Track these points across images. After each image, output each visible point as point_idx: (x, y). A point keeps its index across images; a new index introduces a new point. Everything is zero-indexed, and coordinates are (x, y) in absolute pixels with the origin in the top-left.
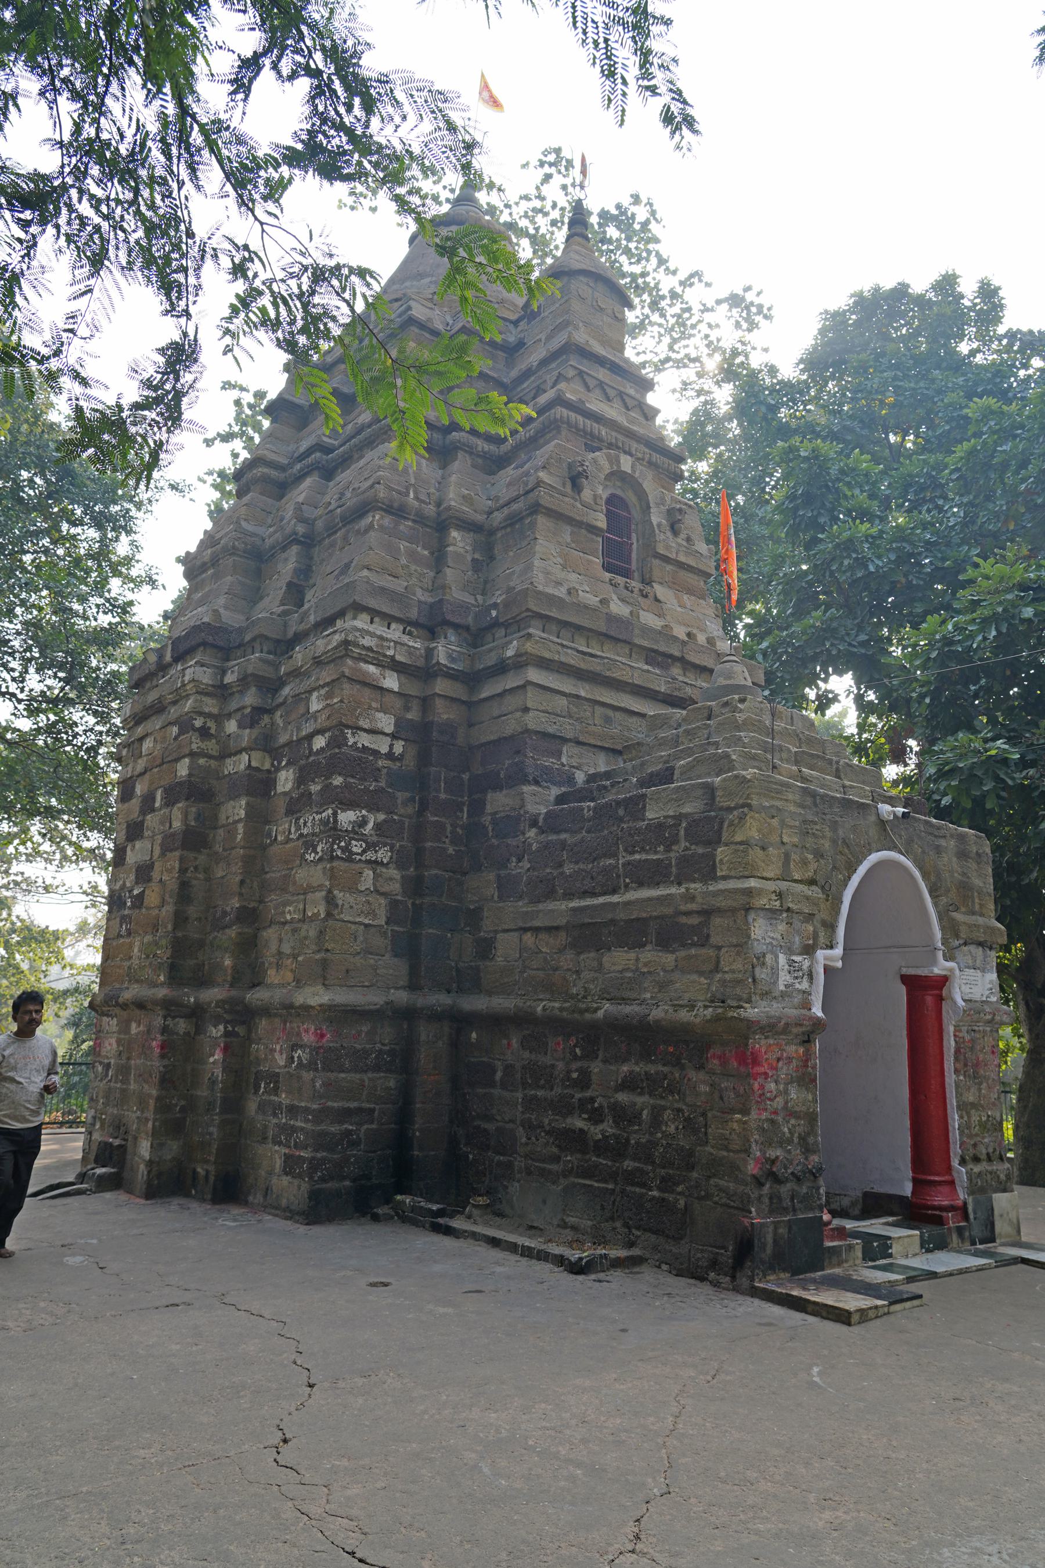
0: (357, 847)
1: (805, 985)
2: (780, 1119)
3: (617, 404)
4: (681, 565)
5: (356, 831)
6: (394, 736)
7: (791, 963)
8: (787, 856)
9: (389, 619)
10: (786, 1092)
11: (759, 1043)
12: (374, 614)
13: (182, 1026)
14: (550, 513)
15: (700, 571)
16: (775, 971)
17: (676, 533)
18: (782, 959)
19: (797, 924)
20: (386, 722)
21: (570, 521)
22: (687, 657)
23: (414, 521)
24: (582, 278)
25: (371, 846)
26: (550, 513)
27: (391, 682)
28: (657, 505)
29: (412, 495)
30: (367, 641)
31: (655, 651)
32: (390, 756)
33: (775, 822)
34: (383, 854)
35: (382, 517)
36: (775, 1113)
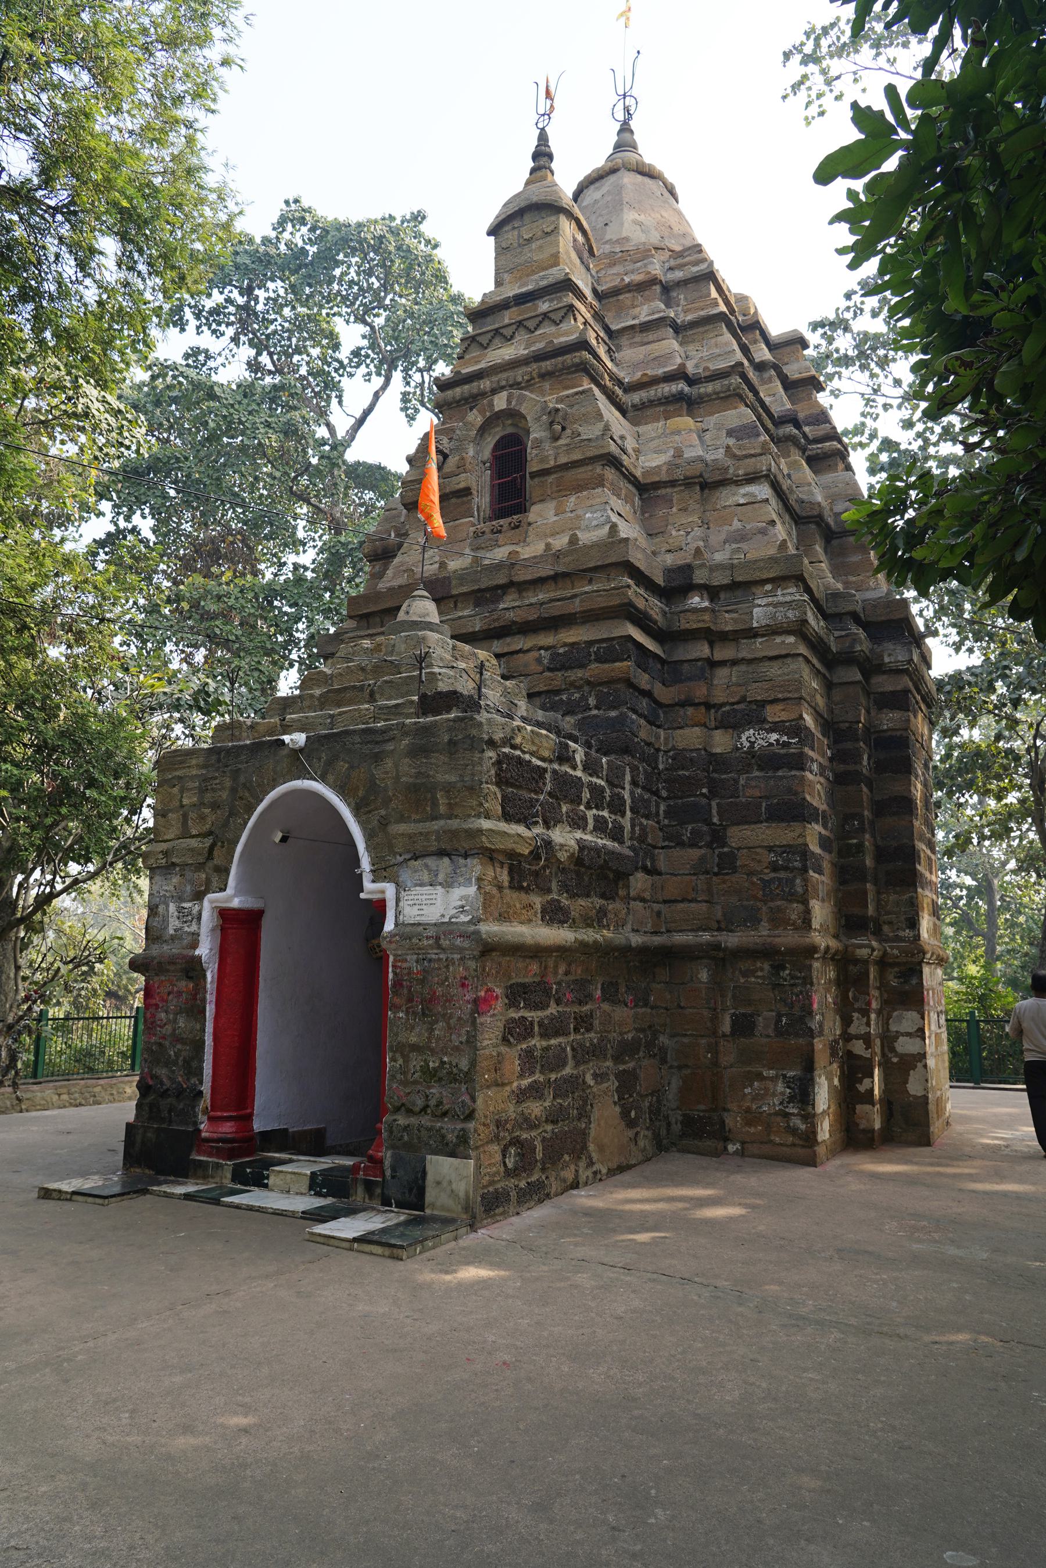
1: (194, 928)
2: (167, 1043)
7: (180, 909)
8: (185, 816)
10: (175, 1021)
15: (591, 458)
18: (172, 907)
19: (189, 874)
22: (516, 579)
24: (506, 228)
31: (479, 590)
33: (175, 790)
36: (164, 1038)
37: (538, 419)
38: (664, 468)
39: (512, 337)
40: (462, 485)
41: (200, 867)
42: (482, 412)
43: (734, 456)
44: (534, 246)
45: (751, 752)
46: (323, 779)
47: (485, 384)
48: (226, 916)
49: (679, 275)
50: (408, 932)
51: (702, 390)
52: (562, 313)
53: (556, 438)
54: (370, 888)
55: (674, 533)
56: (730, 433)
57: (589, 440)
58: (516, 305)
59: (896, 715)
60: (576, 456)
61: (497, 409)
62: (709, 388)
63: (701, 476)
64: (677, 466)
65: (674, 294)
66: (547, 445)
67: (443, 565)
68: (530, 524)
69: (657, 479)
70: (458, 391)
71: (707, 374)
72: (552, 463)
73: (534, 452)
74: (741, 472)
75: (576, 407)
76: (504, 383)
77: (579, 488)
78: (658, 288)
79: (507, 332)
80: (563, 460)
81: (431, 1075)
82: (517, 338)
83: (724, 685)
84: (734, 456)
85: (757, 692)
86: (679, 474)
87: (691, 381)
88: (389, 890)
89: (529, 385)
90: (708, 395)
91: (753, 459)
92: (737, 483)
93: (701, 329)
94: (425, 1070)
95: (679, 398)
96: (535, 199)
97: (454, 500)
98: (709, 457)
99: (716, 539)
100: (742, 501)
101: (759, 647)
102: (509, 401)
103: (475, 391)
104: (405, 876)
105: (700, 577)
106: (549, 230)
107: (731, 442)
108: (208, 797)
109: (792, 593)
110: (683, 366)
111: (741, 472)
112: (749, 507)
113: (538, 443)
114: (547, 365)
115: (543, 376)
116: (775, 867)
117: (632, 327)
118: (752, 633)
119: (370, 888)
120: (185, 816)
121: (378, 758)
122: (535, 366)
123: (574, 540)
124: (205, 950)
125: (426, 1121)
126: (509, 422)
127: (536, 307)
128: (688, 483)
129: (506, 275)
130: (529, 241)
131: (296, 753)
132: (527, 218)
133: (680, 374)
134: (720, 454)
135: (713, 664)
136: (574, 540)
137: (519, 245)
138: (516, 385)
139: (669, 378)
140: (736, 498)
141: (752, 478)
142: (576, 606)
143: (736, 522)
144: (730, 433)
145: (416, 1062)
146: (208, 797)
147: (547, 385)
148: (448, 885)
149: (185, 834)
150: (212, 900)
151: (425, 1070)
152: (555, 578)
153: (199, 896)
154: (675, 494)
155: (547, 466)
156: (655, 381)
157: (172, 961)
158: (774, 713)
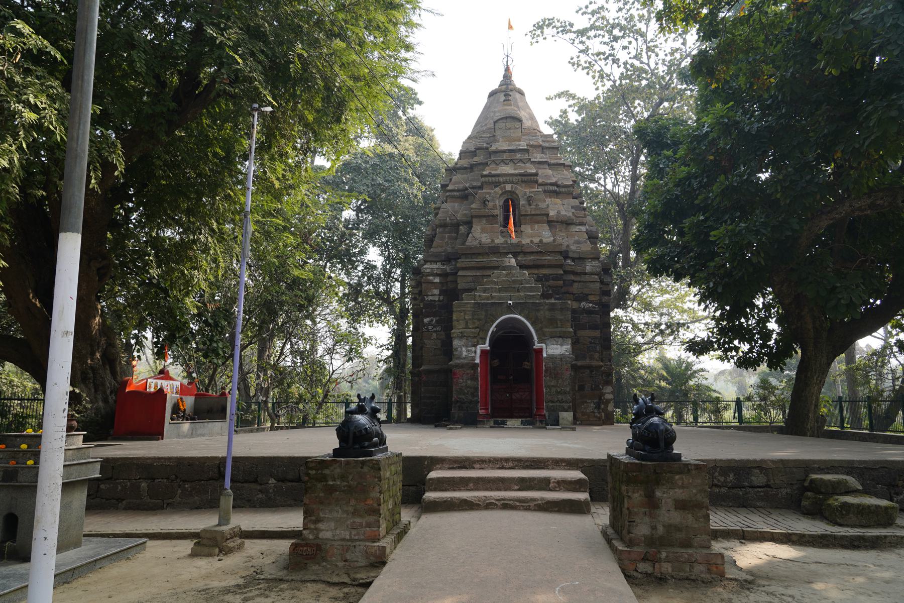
0: (430, 328)
1: (473, 355)
3: (511, 164)
5: (430, 323)
6: (440, 295)
8: (467, 323)
9: (436, 262)
11: (457, 371)
12: (431, 262)
13: (417, 379)
14: (476, 217)
16: (461, 352)
17: (530, 205)
18: (464, 349)
20: (436, 292)
21: (484, 216)
25: (434, 327)
26: (476, 217)
27: (437, 280)
30: (428, 271)
32: (439, 300)
34: (439, 328)
41: (475, 337)
42: (501, 189)
45: (584, 309)
46: (520, 314)
47: (501, 179)
48: (483, 351)
49: (547, 145)
50: (552, 358)
53: (530, 205)
54: (537, 345)
56: (572, 207)
59: (606, 298)
62: (563, 190)
66: (527, 207)
67: (493, 241)
70: (490, 179)
77: (538, 222)
81: (558, 393)
83: (576, 288)
85: (586, 291)
86: (560, 219)
87: (558, 186)
88: (544, 346)
89: (517, 183)
92: (576, 224)
94: (556, 391)
95: (555, 192)
99: (571, 241)
101: (587, 278)
104: (548, 342)
105: (571, 255)
108: (476, 317)
109: (596, 263)
113: (523, 205)
114: (524, 178)
116: (591, 343)
118: (585, 274)
119: (537, 345)
120: (467, 323)
121: (538, 310)
123: (541, 241)
124: (478, 361)
125: (558, 404)
128: (562, 222)
131: (509, 306)
132: (508, 120)
133: (555, 184)
134: (571, 214)
135: (574, 281)
136: (541, 241)
138: (512, 182)
139: (551, 184)
141: (581, 224)
142: (546, 263)
144: (572, 207)
145: (554, 390)
146: (476, 317)
148: (561, 345)
149: (467, 327)
150: (479, 348)
151: (556, 391)
152: (538, 253)
153: (475, 346)
154: (558, 225)
156: (547, 184)
157: (467, 364)
158: (591, 298)
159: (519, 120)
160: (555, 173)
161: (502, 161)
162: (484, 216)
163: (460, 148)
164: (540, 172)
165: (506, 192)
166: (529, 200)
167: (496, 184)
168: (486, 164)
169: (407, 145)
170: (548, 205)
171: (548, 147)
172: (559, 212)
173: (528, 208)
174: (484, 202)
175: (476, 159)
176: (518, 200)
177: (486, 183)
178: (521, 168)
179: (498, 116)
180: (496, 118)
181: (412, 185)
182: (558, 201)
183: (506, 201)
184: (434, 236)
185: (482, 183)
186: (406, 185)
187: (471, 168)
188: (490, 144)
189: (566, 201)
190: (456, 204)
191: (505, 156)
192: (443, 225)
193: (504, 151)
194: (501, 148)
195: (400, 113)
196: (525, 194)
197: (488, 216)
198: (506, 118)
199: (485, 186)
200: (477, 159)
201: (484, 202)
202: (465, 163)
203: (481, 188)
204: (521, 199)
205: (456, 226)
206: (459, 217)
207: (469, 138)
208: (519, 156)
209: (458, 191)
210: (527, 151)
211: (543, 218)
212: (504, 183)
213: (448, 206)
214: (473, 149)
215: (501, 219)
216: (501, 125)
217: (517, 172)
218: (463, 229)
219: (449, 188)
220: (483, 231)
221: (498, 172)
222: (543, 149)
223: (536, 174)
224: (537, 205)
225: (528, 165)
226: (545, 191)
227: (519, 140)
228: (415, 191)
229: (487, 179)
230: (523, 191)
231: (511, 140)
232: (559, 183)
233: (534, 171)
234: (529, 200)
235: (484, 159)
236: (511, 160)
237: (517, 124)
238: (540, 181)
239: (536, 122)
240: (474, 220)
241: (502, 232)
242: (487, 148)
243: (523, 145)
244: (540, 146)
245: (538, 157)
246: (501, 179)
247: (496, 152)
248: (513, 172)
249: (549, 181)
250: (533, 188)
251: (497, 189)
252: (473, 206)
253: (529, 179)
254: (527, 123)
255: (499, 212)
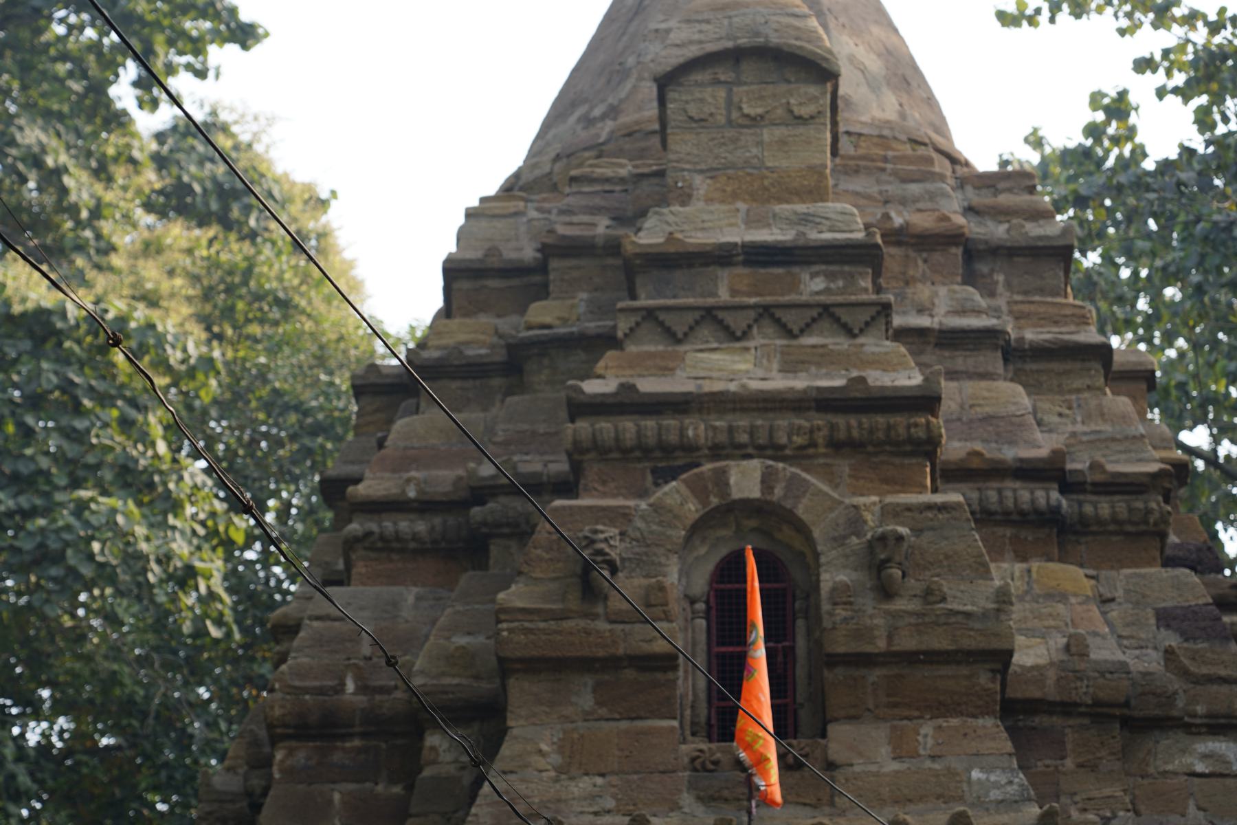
4: (911, 658)
14: (534, 666)
17: (886, 592)
21: (586, 665)
23: (364, 735)
26: (534, 666)
28: (840, 541)
29: (350, 686)
35: (291, 752)
37: (840, 541)
38: (1052, 675)
39: (745, 335)
40: (660, 646)
42: (699, 490)
43: (1185, 673)
44: (766, 134)
47: (696, 429)
49: (998, 231)
51: (1088, 509)
52: (865, 316)
53: (886, 592)
55: (1075, 814)
56: (1165, 618)
57: (968, 615)
58: (747, 263)
60: (939, 641)
61: (736, 494)
62: (1104, 507)
63: (1127, 704)
64: (1079, 676)
65: (983, 268)
68: (831, 766)
69: (1036, 694)
70: (629, 426)
71: (1099, 477)
72: (882, 645)
73: (841, 612)
74: (1200, 709)
75: (928, 536)
76: (744, 438)
77: (941, 707)
78: (958, 251)
79: (737, 322)
80: (908, 642)
82: (756, 341)
84: (1185, 673)
86: (1082, 692)
87: (1069, 484)
89: (800, 456)
90: (1099, 521)
91: (1225, 689)
93: (1056, 366)
95: (1049, 519)
96: (775, 40)
97: (629, 674)
98: (1136, 666)
100: (1200, 768)
102: (767, 480)
103: (673, 438)
106: (805, 111)
107: (1171, 639)
110: (1058, 456)
111: (1200, 709)
112: (1213, 781)
113: (842, 595)
115: (837, 446)
117: (922, 332)
122: (819, 420)
126: (753, 523)
127: (794, 286)
129: (698, 180)
130: (755, 121)
132: (749, 69)
133: (1047, 471)
134: (1151, 662)
137: (730, 123)
138: (771, 449)
139: (1028, 472)
140: (1188, 760)
143: (1192, 809)
144: (1165, 618)
147: (844, 466)
155: (869, 649)
156: (996, 471)
159: (820, 71)
160: (1050, 407)
161: (710, 315)
162: (586, 665)
163: (449, 246)
164: (948, 388)
165: (731, 512)
166: (881, 561)
167: (668, 460)
168: (610, 341)
169: (147, 273)
170: (1003, 598)
171: (1010, 234)
172: (1075, 648)
173: (874, 615)
174: (588, 579)
175: (545, 314)
176: (811, 562)
177: (600, 450)
178: (823, 358)
179: (680, 39)
180: (673, 58)
181: (162, 505)
182: (1071, 576)
183: (731, 569)
184: (256, 807)
185: (578, 454)
186: (125, 511)
187: (513, 365)
188: (632, 218)
189: (1121, 579)
190: (410, 595)
191: (724, 288)
192: (317, 726)
193: (722, 257)
194: (699, 238)
195: (123, 92)
196: (855, 522)
197: (613, 663)
198: (735, 56)
199: (592, 471)
200: (545, 314)
201: (587, 568)
202: (479, 336)
203: (567, 487)
204: (829, 554)
205: (398, 731)
206: (423, 668)
207: (512, 187)
208: (813, 285)
209: (424, 506)
210: (861, 255)
211: (967, 674)
212: (717, 452)
213: (358, 601)
214: (528, 253)
215: (691, 683)
216: (704, 97)
217: (800, 383)
218: (442, 748)
219: (371, 487)
220: (575, 760)
221: (678, 384)
222: (973, 258)
223: (926, 401)
224: (930, 595)
225: (875, 344)
226: (984, 517)
227: (817, 193)
228: (181, 548)
229: (606, 427)
230: (840, 505)
231: (765, 191)
232: (1078, 464)
233: (910, 379)
234: (881, 561)
235: (599, 310)
236: (766, 312)
237: (805, 97)
238: (953, 449)
239: (930, 101)
240: (520, 690)
241: (699, 766)
242: (613, 247)
243: (844, 217)
244: (954, 238)
245: (941, 302)
246: (696, 429)
247: (676, 261)
248: (778, 383)
249: (1009, 454)
250: (905, 485)
251: (673, 492)
252: (515, 596)
253: (881, 432)
254: (869, 105)
255: (684, 635)
